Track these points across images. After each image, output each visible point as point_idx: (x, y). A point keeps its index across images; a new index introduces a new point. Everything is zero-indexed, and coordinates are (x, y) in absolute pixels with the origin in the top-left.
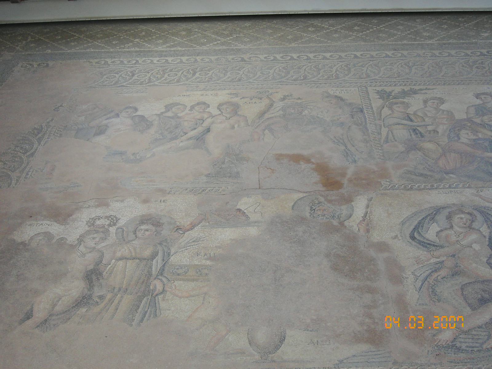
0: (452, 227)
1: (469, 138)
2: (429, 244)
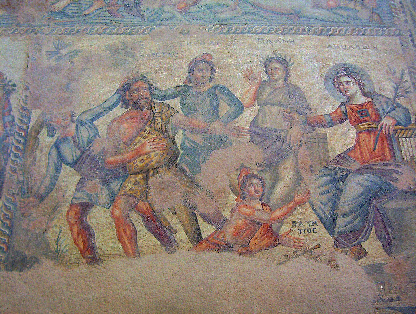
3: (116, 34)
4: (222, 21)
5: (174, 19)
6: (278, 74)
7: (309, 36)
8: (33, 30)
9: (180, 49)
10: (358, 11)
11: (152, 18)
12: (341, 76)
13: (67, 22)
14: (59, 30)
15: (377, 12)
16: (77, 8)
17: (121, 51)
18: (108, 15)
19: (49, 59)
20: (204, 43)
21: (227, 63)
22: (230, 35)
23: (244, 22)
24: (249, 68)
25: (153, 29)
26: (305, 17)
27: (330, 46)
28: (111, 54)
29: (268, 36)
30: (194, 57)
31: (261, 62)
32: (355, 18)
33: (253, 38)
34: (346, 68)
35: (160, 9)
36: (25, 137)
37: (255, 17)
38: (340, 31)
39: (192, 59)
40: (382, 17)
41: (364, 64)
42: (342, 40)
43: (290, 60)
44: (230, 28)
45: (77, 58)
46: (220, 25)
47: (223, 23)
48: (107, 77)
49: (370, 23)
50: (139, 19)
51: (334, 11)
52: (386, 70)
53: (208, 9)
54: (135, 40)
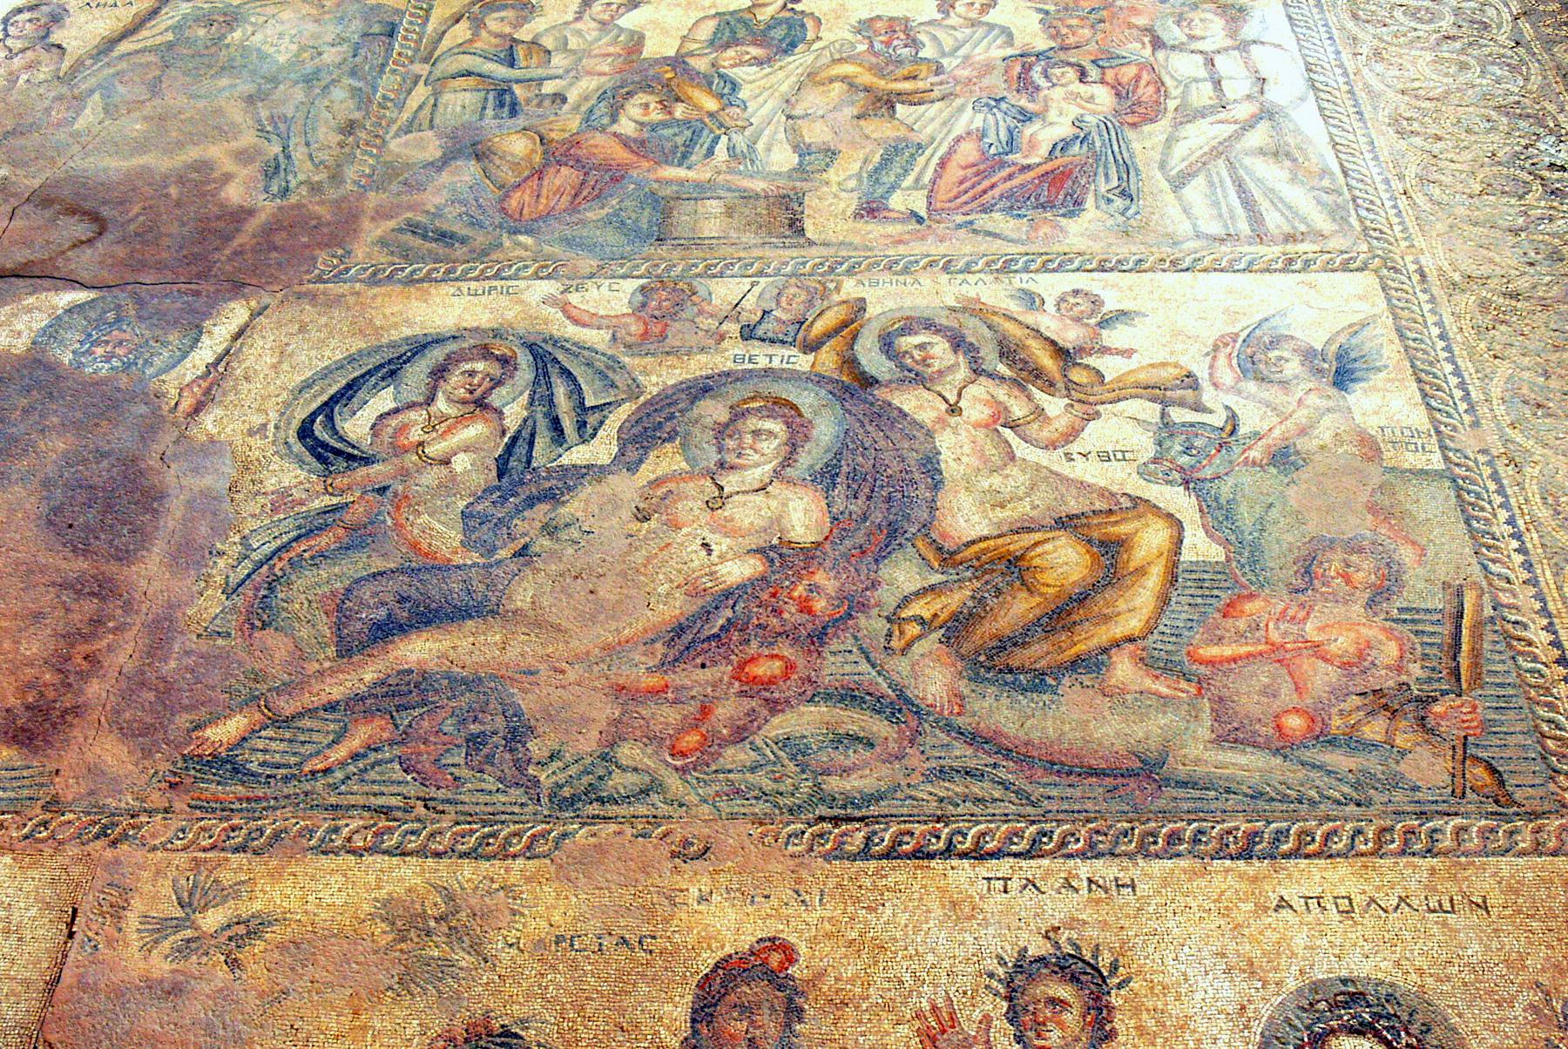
0: (430, 400)
1: (646, 119)
2: (338, 452)
3: (421, 852)
4: (844, 807)
5: (655, 798)
6: (1061, 1025)
7: (1197, 864)
8: (106, 827)
9: (666, 921)
10: (1403, 753)
11: (566, 792)
12: (1333, 1031)
13: (240, 799)
14: (203, 829)
15: (1484, 755)
16: (283, 746)
17: (432, 924)
18: (399, 774)
19: (147, 949)
20: (767, 897)
21: (851, 981)
22: (872, 865)
23: (932, 807)
24: (940, 1002)
25: (565, 835)
26: (1183, 784)
27: (1283, 904)
28: (390, 937)
29: (1023, 863)
30: (720, 954)
31: (991, 975)
32: (1394, 782)
33: (962, 874)
34: (1356, 998)
35: (604, 757)
37: (977, 789)
38: (1327, 837)
39: (712, 962)
40: (1505, 776)
41: (1430, 980)
42: (1338, 878)
43: (1114, 967)
44: (875, 833)
45: (260, 945)
46: (836, 820)
47: (845, 813)
48: (364, 1028)
49: (1452, 800)
50: (516, 794)
51: (1307, 755)
52: (1532, 1006)
53: (793, 757)
54: (493, 881)
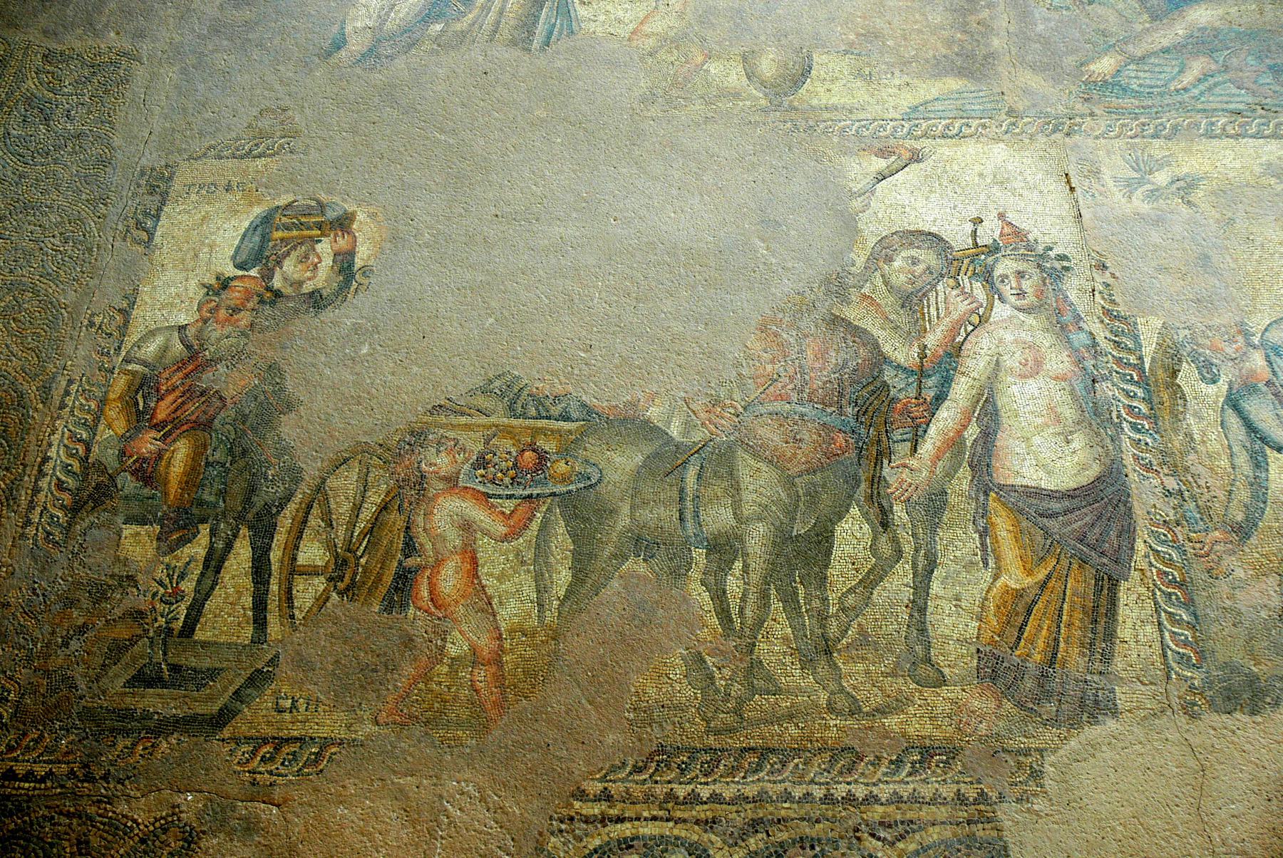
36: (1143, 382)
